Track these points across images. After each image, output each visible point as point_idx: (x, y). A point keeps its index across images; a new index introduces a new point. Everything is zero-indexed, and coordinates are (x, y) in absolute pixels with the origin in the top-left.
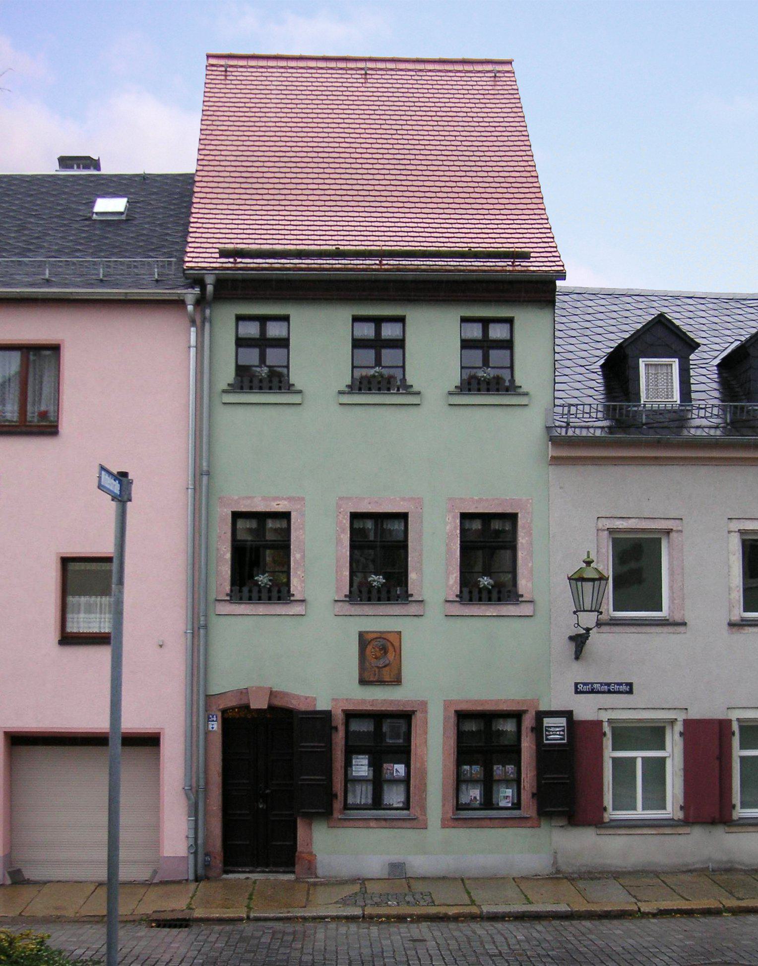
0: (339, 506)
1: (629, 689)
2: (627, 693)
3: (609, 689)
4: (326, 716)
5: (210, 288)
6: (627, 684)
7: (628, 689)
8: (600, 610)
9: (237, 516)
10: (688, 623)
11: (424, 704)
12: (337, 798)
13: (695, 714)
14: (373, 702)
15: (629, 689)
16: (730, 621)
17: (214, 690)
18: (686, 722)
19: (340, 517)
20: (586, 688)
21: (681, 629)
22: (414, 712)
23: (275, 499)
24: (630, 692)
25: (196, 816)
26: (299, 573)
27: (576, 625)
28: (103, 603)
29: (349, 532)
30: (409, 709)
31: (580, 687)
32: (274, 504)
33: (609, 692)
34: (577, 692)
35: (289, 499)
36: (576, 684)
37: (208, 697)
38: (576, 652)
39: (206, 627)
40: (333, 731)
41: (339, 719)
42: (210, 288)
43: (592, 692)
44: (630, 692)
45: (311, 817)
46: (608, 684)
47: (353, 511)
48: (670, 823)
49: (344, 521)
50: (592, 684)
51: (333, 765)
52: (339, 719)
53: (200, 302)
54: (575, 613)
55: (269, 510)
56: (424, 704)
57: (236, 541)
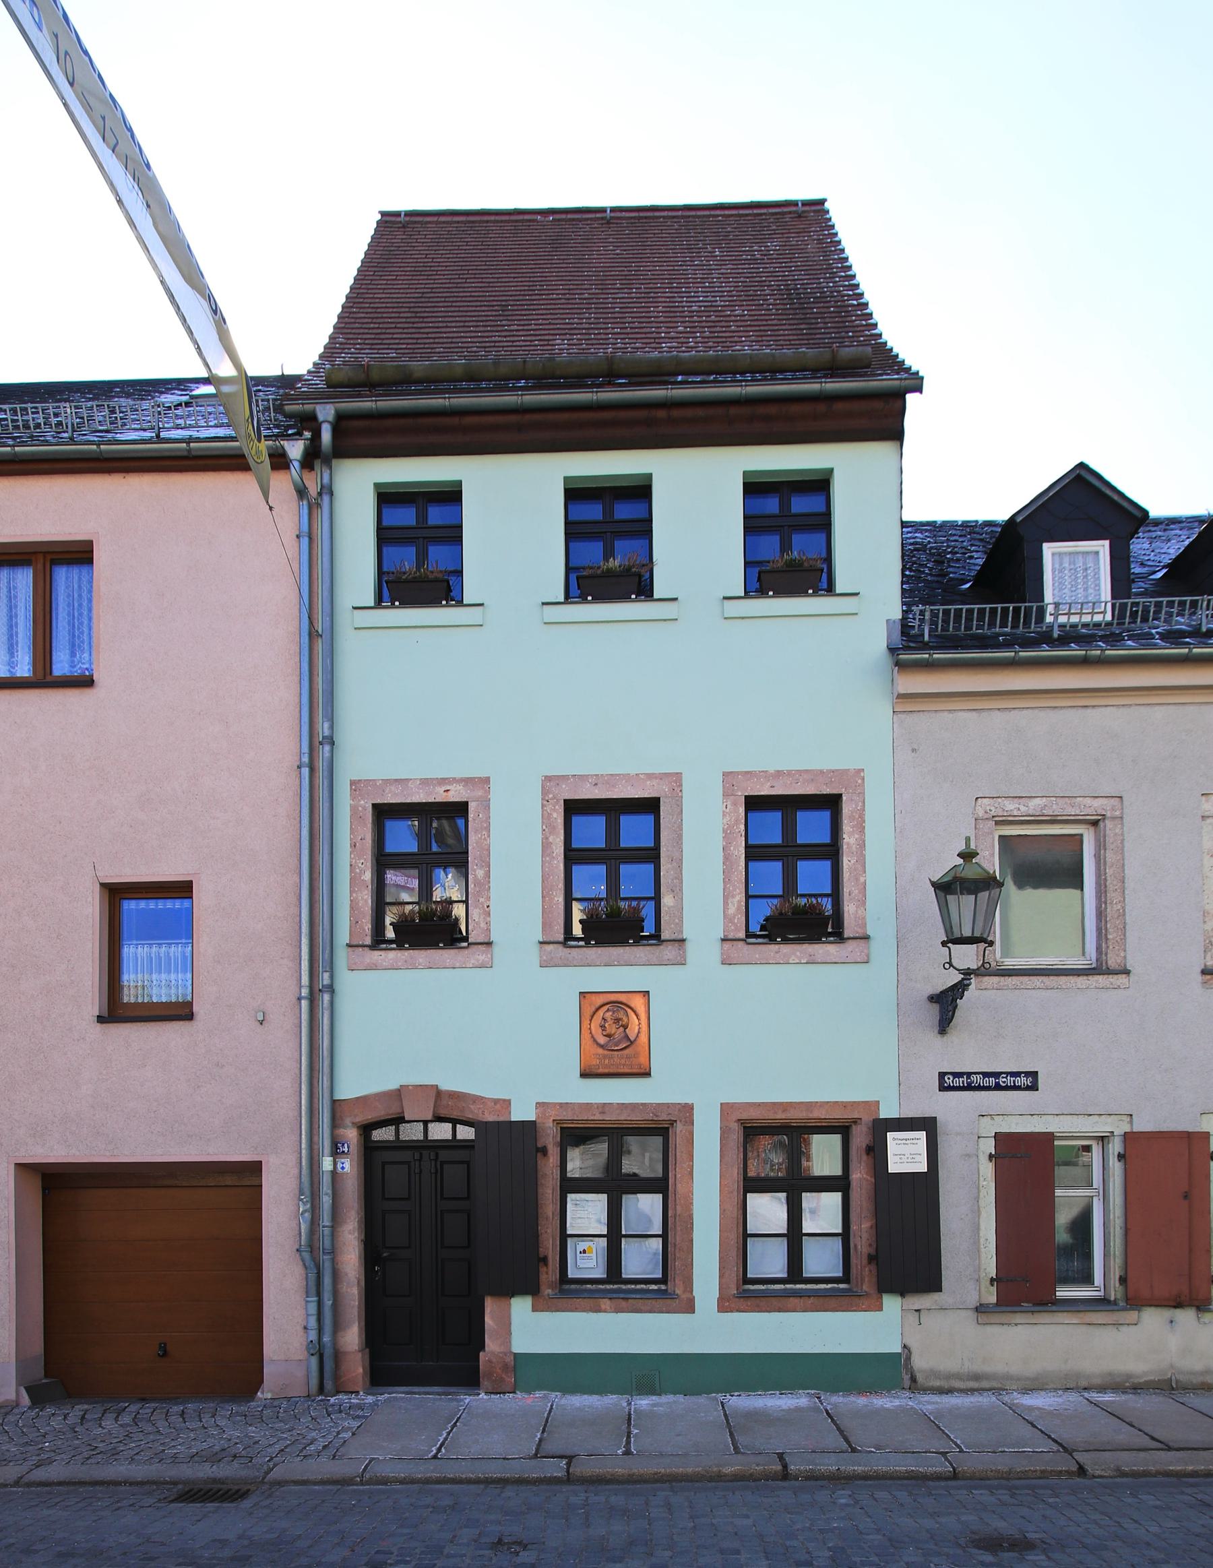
0: (545, 792)
1: (1032, 1081)
2: (1028, 1088)
3: (996, 1082)
4: (528, 1128)
5: (326, 436)
6: (1027, 1074)
7: (1029, 1081)
8: (989, 939)
9: (384, 813)
10: (1133, 971)
11: (688, 1109)
12: (546, 1264)
13: (1144, 1124)
14: (604, 1107)
15: (1032, 1081)
16: (1205, 965)
17: (348, 1089)
18: (1128, 1137)
19: (548, 808)
20: (959, 1082)
21: (1121, 980)
22: (672, 1123)
23: (443, 781)
24: (1034, 1087)
25: (319, 1294)
26: (482, 900)
27: (947, 966)
28: (172, 955)
29: (562, 832)
30: (664, 1117)
31: (949, 1080)
32: (441, 790)
33: (998, 1087)
34: (943, 1088)
35: (467, 781)
36: (942, 1075)
37: (335, 1103)
38: (941, 1021)
39: (331, 989)
40: (105, 1014)
41: (550, 1138)
42: (326, 436)
43: (969, 1087)
44: (1034, 1087)
45: (509, 1291)
46: (996, 1075)
47: (567, 798)
48: (1102, 1303)
49: (555, 815)
50: (969, 1074)
51: (540, 1211)
52: (550, 1138)
53: (311, 458)
54: (944, 944)
55: (433, 800)
56: (688, 1109)
57: (382, 855)
